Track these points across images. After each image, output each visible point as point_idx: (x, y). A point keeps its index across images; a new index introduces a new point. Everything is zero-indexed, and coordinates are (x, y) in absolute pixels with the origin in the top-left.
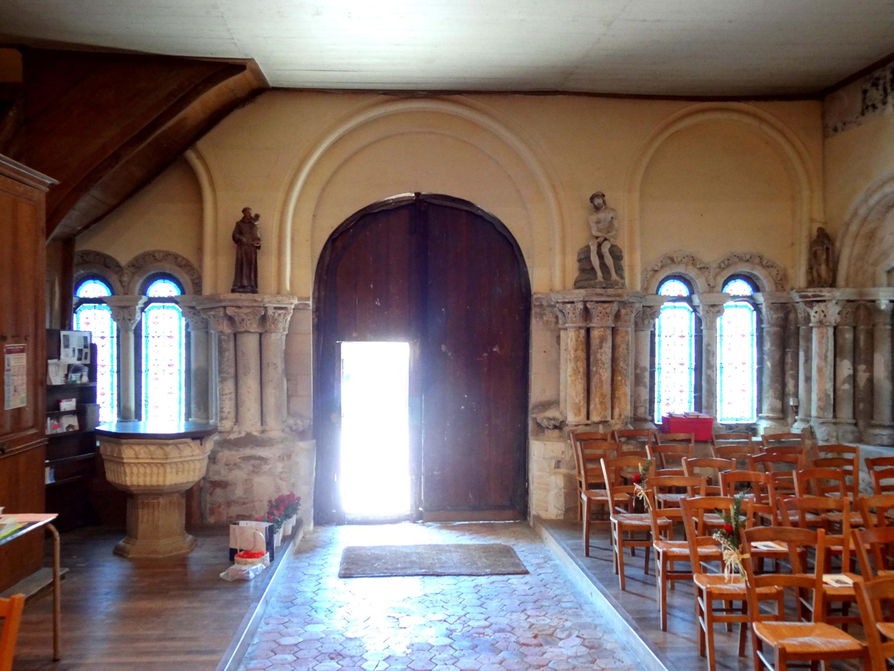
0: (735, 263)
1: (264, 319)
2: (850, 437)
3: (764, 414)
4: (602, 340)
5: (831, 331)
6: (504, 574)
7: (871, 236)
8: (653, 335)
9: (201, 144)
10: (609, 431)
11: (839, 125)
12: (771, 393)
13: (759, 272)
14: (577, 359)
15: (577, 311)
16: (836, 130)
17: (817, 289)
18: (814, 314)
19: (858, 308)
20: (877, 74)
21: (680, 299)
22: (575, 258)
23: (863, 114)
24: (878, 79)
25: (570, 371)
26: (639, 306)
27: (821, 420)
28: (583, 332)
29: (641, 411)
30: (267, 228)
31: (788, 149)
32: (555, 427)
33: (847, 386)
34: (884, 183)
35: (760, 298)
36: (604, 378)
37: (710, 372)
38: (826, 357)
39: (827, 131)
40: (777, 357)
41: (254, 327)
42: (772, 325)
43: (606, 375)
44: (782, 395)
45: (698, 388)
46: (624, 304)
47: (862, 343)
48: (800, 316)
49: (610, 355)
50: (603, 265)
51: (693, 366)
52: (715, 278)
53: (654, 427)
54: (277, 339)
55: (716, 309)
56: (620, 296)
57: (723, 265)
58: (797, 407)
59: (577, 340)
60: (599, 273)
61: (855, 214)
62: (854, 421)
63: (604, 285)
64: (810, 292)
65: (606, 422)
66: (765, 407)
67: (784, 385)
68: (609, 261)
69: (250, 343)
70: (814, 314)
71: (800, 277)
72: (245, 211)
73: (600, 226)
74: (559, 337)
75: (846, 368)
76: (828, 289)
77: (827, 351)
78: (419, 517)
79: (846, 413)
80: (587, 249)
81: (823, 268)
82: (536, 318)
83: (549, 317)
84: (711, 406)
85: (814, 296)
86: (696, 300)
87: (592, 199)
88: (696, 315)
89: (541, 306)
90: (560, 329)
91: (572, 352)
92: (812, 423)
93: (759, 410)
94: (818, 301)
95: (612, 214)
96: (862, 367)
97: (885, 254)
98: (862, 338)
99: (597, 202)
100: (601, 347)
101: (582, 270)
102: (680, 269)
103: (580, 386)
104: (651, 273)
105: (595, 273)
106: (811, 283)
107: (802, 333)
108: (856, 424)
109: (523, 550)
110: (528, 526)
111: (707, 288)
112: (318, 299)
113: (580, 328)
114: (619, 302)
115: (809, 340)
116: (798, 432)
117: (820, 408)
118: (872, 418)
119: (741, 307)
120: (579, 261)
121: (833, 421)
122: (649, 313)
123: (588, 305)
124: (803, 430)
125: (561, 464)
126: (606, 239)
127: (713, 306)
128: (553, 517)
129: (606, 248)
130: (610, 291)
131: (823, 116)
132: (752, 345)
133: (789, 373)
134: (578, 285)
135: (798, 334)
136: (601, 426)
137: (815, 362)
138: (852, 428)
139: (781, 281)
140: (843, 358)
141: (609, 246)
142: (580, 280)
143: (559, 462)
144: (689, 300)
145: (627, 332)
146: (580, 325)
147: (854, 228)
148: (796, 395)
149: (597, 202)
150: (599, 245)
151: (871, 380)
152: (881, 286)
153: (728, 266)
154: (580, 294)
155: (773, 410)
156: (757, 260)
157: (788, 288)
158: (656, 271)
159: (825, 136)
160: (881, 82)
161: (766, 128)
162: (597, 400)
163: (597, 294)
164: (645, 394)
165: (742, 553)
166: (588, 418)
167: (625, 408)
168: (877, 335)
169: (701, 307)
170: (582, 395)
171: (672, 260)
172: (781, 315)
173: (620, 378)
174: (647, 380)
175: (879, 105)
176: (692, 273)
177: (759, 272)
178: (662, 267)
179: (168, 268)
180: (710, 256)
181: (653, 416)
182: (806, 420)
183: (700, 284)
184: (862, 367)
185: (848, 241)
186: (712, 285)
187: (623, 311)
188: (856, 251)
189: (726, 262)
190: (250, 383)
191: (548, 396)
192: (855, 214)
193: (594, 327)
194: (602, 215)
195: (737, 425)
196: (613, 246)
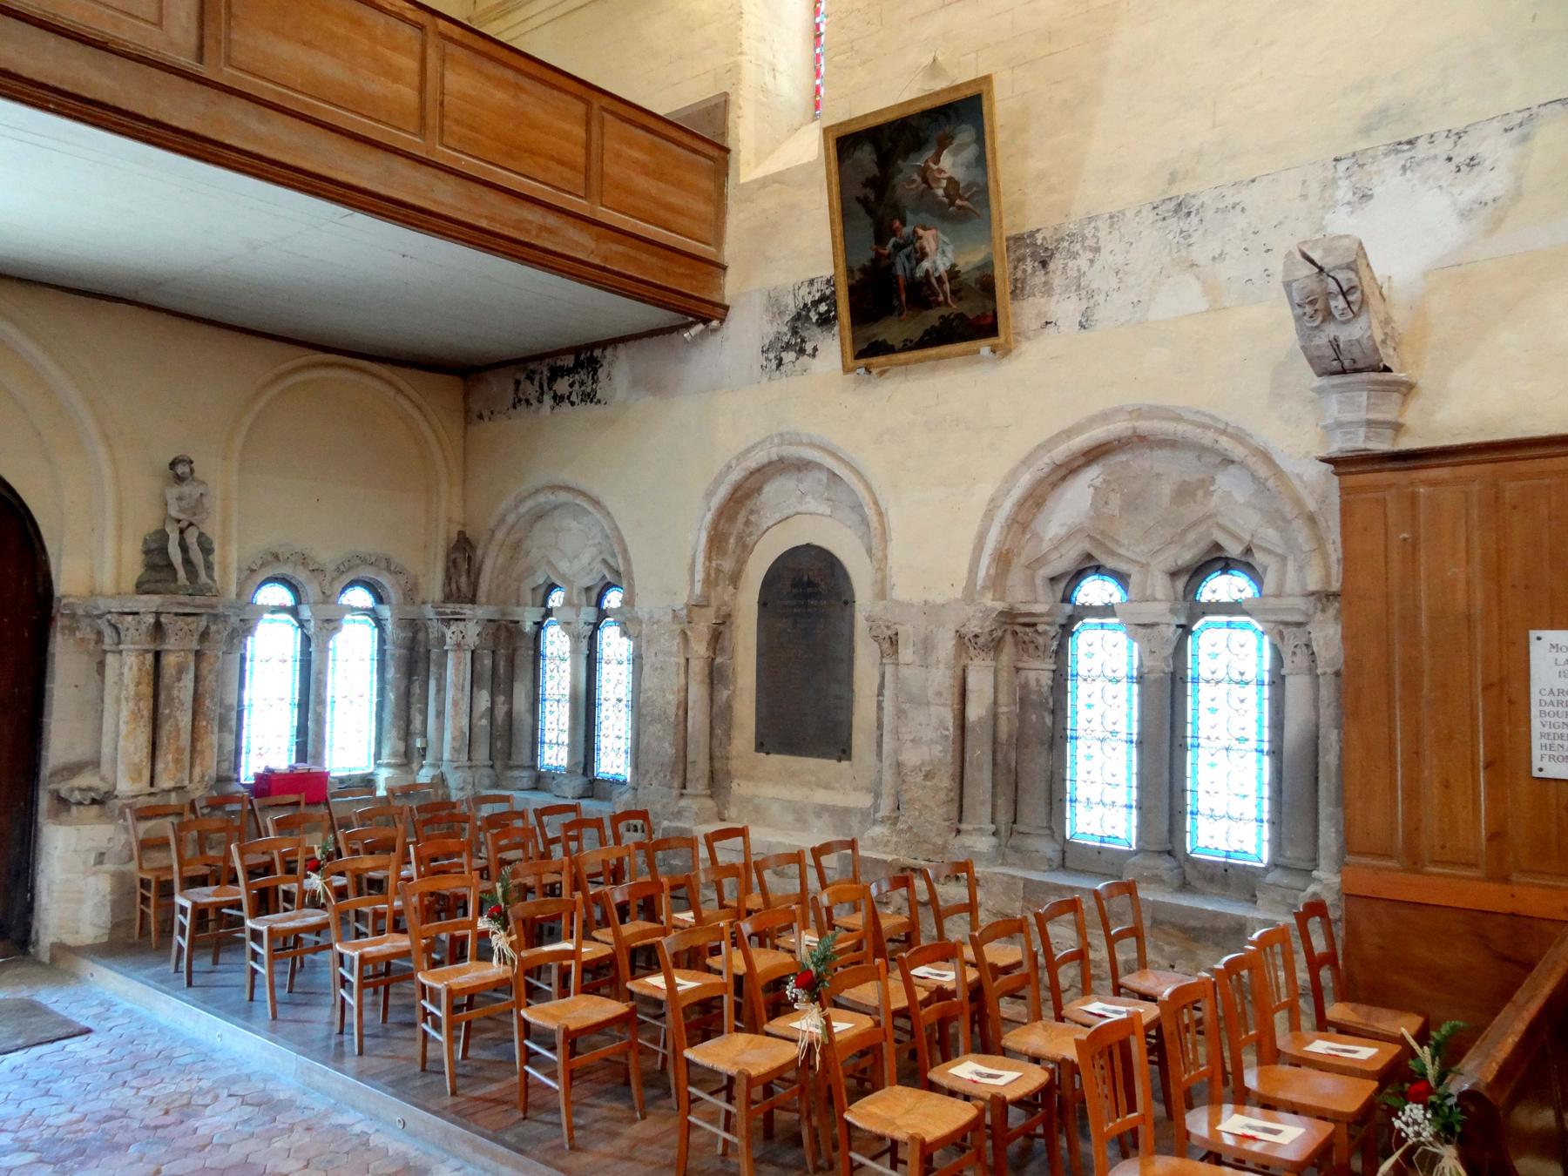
0: (357, 566)
2: (487, 782)
3: (384, 760)
4: (181, 669)
6: (52, 1041)
7: (517, 546)
8: (243, 659)
10: (186, 800)
11: (486, 413)
12: (394, 733)
13: (385, 580)
14: (138, 697)
15: (143, 628)
16: (481, 417)
17: (458, 606)
18: (451, 635)
19: (499, 628)
20: (532, 366)
21: (281, 609)
22: (139, 545)
23: (514, 407)
24: (533, 372)
25: (125, 715)
27: (456, 764)
28: (150, 657)
31: (424, 426)
32: (94, 801)
33: (484, 722)
34: (537, 491)
35: (385, 612)
36: (182, 724)
37: (318, 709)
38: (463, 687)
39: (471, 417)
40: (402, 688)
42: (399, 646)
43: (185, 719)
44: (407, 735)
45: (302, 731)
46: (215, 617)
47: (501, 670)
48: (431, 636)
49: (192, 692)
50: (187, 562)
51: (296, 701)
52: (331, 584)
53: (242, 789)
55: (331, 624)
56: (212, 606)
57: (342, 568)
58: (424, 749)
59: (140, 670)
60: (181, 573)
61: (502, 520)
62: (491, 763)
63: (190, 591)
64: (450, 607)
65: (182, 788)
66: (386, 751)
67: (408, 722)
70: (451, 635)
73: (184, 504)
74: (101, 665)
76: (470, 606)
77: (464, 680)
79: (482, 754)
80: (162, 535)
81: (464, 579)
82: (63, 634)
83: (85, 632)
84: (319, 756)
85: (453, 613)
86: (306, 612)
87: (173, 465)
88: (303, 633)
89: (73, 616)
90: (105, 652)
91: (132, 688)
92: (443, 769)
93: (378, 756)
94: (457, 620)
95: (201, 490)
96: (501, 699)
97: (531, 571)
98: (502, 663)
99: (179, 470)
100: (179, 680)
101: (150, 567)
102: (286, 570)
103: (143, 738)
104: (247, 573)
105: (175, 571)
106: (448, 598)
107: (433, 656)
108: (492, 767)
109: (52, 997)
110: (38, 963)
111: (321, 596)
113: (147, 651)
114: (210, 615)
115: (442, 666)
116: (426, 780)
117: (455, 750)
118: (509, 756)
119: (360, 623)
120: (147, 552)
121: (468, 764)
123: (163, 619)
124: (433, 778)
125: (106, 857)
126: (191, 524)
127: (328, 621)
128: (89, 941)
130: (199, 600)
131: (466, 397)
132: (371, 672)
133: (416, 706)
134: (141, 588)
135: (428, 658)
136: (173, 795)
137: (450, 694)
138: (488, 771)
139: (411, 592)
140: (480, 689)
141: (196, 534)
142: (148, 582)
143: (102, 854)
144: (294, 611)
145: (217, 657)
146: (147, 647)
147: (500, 535)
148: (424, 734)
149: (179, 470)
150: (182, 532)
151: (510, 713)
152: (525, 605)
153: (350, 568)
154: (149, 603)
155: (394, 754)
156: (384, 564)
157: (418, 600)
158: (253, 571)
159: (468, 421)
160: (537, 378)
161: (402, 400)
162: (170, 757)
163: (181, 604)
165: (509, 935)
166: (152, 784)
168: (518, 660)
169: (312, 623)
170: (145, 750)
171: (276, 557)
172: (410, 634)
173: (204, 723)
174: (233, 723)
175: (534, 402)
176: (301, 576)
177: (385, 580)
178: (262, 565)
180: (327, 555)
181: (238, 773)
182: (435, 766)
183: (311, 590)
184: (501, 699)
185: (493, 551)
186: (328, 593)
187: (213, 628)
188: (500, 561)
189: (346, 564)
191: (80, 753)
192: (502, 520)
193: (168, 651)
194: (186, 489)
195: (350, 777)
196: (201, 535)
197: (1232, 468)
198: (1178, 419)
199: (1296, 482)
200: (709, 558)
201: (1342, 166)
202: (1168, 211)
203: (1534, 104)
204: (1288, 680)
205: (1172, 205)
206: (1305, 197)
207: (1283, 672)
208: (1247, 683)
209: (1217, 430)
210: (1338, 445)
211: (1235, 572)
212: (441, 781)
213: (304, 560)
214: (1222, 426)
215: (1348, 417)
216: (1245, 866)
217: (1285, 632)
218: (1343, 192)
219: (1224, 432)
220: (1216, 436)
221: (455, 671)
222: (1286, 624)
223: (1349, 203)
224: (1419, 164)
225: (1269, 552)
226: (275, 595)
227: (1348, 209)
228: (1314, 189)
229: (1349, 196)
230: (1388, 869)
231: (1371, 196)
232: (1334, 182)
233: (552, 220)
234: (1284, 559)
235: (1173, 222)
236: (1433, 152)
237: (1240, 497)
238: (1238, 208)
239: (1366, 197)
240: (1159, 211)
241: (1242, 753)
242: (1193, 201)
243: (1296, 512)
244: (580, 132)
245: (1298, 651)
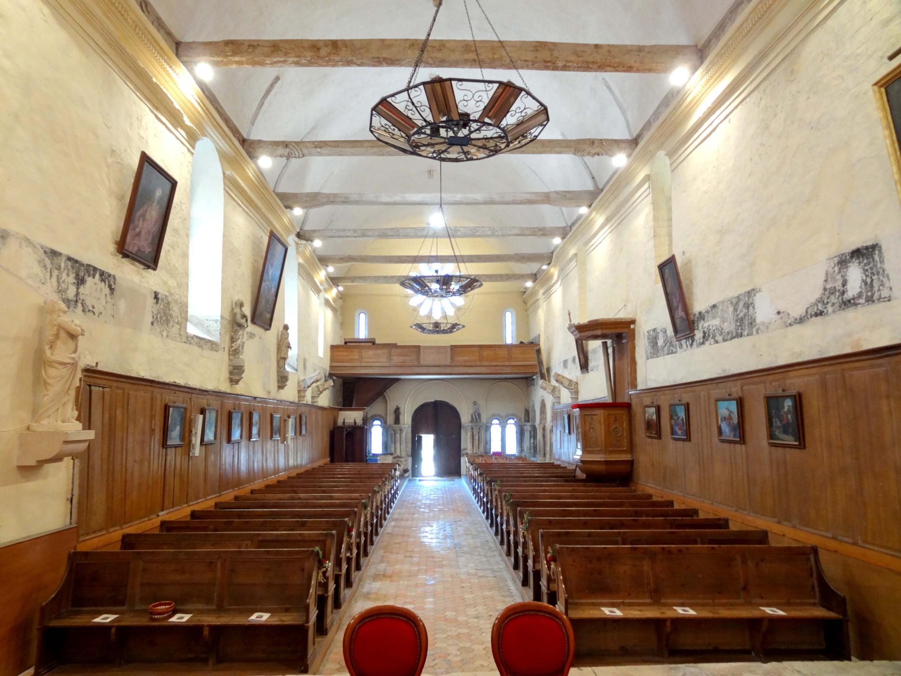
1: (401, 430)
4: (476, 435)
5: (529, 433)
9: (387, 391)
18: (525, 427)
26: (484, 426)
29: (487, 451)
30: (401, 410)
41: (399, 432)
46: (480, 426)
54: (404, 434)
68: (477, 417)
69: (398, 435)
71: (523, 420)
72: (397, 406)
75: (532, 441)
78: (435, 476)
79: (532, 451)
99: (475, 403)
103: (471, 444)
112: (412, 425)
122: (488, 428)
129: (476, 414)
139: (520, 420)
154: (470, 424)
164: (488, 447)
167: (482, 449)
179: (378, 418)
183: (502, 421)
190: (398, 445)
191: (465, 447)
200: (541, 415)
212: (525, 455)
213: (499, 415)
221: (527, 435)
226: (495, 421)
233: (501, 368)
244: (507, 352)
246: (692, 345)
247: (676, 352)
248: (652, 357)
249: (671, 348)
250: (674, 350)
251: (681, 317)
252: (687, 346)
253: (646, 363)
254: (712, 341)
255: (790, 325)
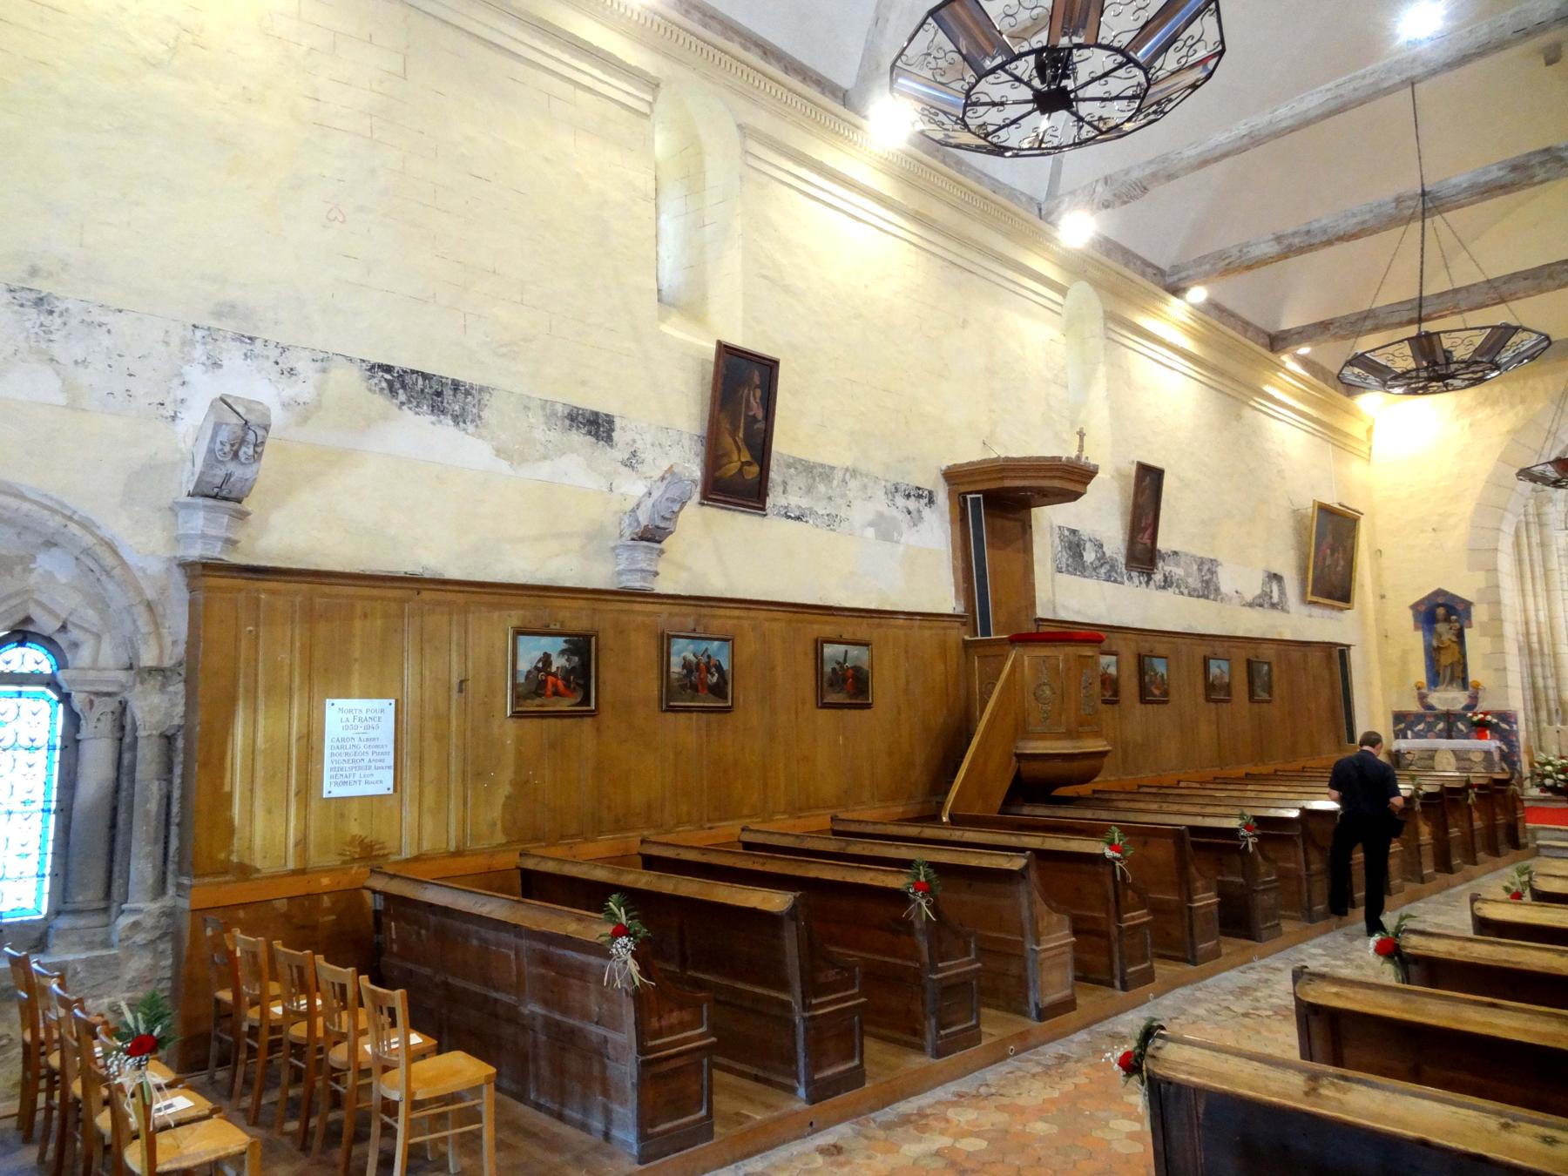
197: (54, 550)
198: (22, 497)
199: (139, 574)
201: (199, 333)
202: (29, 300)
203: (331, 351)
204: (84, 746)
205: (33, 296)
206: (167, 343)
207: (79, 737)
208: (38, 749)
209: (64, 516)
210: (195, 552)
211: (34, 646)
214: (68, 513)
215: (212, 532)
216: (22, 922)
217: (97, 701)
218: (199, 352)
219: (70, 518)
220: (63, 521)
222: (97, 694)
223: (203, 364)
224: (257, 357)
225: (86, 630)
227: (203, 368)
228: (175, 342)
229: (204, 358)
230: (226, 883)
231: (220, 366)
232: (192, 343)
234: (98, 637)
235: (32, 313)
236: (265, 353)
237: (62, 578)
238: (104, 328)
239: (217, 365)
240: (17, 295)
241: (26, 816)
242: (56, 303)
243: (138, 600)
245: (102, 718)
246: (1147, 583)
247: (1122, 583)
248: (1068, 572)
249: (1113, 574)
250: (1119, 579)
251: (1145, 544)
252: (1140, 583)
253: (1053, 580)
254: (1177, 591)
255: (1244, 605)
